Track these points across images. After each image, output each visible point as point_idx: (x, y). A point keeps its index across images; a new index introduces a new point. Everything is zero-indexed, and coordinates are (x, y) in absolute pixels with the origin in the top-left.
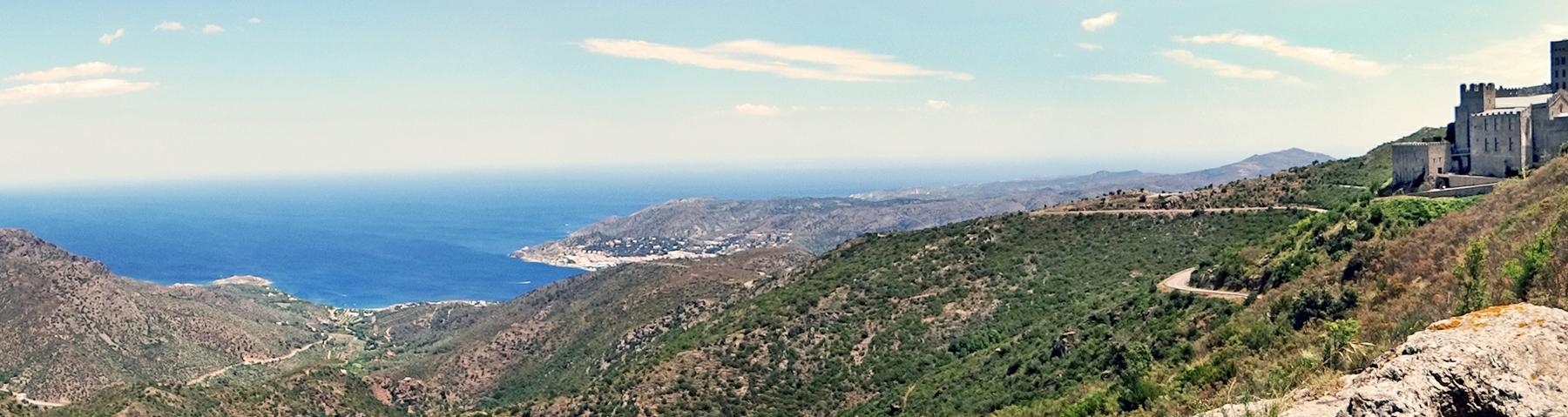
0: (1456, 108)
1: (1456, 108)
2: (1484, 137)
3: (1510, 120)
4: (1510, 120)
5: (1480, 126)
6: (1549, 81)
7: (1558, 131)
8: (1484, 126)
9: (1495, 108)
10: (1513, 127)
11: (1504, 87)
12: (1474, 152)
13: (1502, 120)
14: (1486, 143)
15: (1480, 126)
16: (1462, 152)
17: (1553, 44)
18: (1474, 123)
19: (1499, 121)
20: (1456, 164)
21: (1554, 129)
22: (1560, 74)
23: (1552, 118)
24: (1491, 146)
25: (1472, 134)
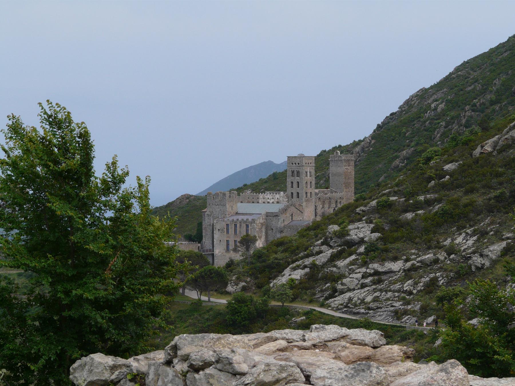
2: (225, 239)
5: (222, 230)
8: (225, 230)
9: (237, 213)
12: (217, 252)
13: (240, 225)
14: (228, 245)
15: (222, 230)
16: (207, 251)
18: (218, 226)
19: (238, 225)
25: (216, 236)
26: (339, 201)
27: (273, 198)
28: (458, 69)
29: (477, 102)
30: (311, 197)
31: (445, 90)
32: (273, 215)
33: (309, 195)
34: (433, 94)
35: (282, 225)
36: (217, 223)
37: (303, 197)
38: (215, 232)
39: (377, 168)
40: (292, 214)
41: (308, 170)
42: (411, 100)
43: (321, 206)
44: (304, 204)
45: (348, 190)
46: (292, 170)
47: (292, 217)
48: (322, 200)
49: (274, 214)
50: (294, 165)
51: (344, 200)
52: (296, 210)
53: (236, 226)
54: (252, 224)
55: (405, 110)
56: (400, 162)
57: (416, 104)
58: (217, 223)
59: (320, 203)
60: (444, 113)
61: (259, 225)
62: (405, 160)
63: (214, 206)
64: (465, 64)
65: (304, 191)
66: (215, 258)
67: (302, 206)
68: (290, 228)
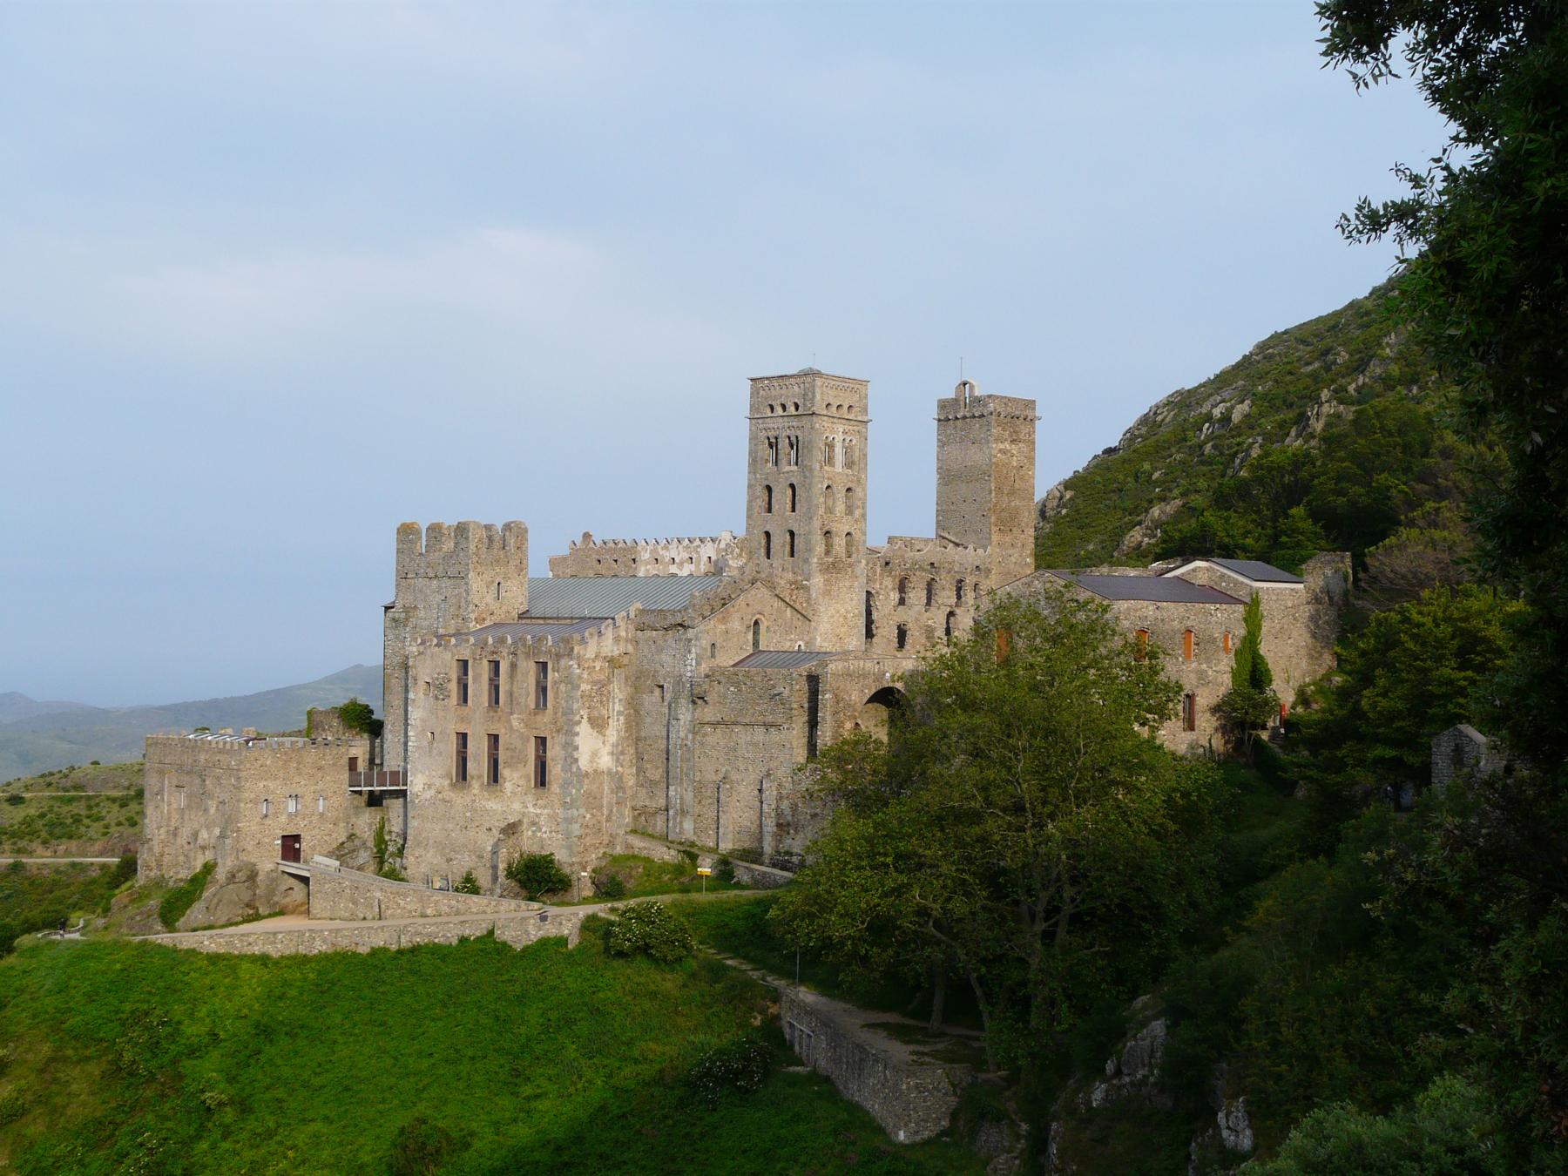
2: (453, 727)
5: (441, 687)
8: (453, 687)
13: (513, 666)
15: (441, 687)
21: (709, 713)
22: (782, 498)
24: (478, 765)
25: (415, 714)
26: (969, 581)
28: (1262, 347)
29: (1350, 384)
31: (1241, 383)
32: (666, 624)
33: (839, 543)
34: (1211, 395)
35: (704, 668)
36: (420, 654)
37: (810, 550)
38: (411, 695)
39: (1082, 552)
40: (756, 623)
41: (839, 438)
42: (1155, 413)
43: (895, 596)
44: (817, 581)
46: (771, 434)
47: (756, 633)
48: (898, 573)
49: (671, 620)
50: (779, 411)
51: (993, 577)
52: (777, 604)
54: (563, 663)
55: (1141, 436)
56: (1145, 535)
57: (1167, 420)
58: (420, 654)
59: (889, 583)
60: (1249, 423)
61: (598, 665)
62: (1156, 529)
63: (421, 582)
64: (1277, 338)
65: (817, 523)
66: (410, 814)
67: (807, 589)
68: (737, 684)
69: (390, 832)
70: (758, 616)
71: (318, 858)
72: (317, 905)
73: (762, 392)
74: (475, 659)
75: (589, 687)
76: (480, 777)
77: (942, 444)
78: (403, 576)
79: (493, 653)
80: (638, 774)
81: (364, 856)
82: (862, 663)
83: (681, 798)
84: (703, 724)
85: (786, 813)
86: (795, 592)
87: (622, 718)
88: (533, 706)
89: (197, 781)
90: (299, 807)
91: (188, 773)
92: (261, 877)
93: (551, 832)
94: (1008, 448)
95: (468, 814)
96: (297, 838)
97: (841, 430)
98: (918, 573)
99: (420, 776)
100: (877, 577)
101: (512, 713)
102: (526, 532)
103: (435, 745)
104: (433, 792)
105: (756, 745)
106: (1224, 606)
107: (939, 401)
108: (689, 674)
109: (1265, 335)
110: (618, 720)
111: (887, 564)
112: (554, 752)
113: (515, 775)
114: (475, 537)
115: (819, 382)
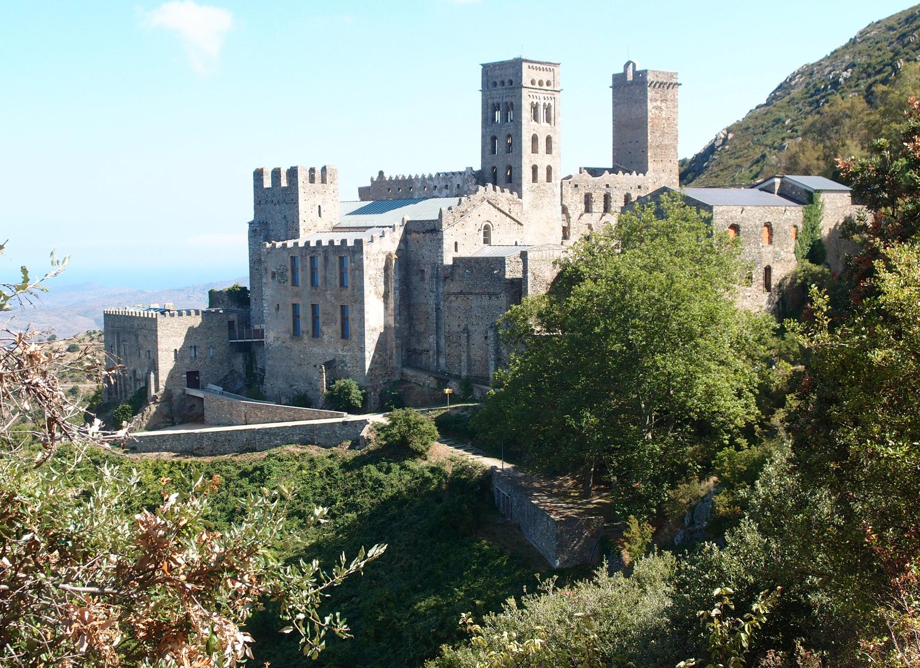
0: (250, 223)
1: (250, 223)
2: (291, 301)
3: (341, 259)
4: (342, 259)
5: (282, 275)
6: (477, 167)
7: (461, 293)
8: (289, 274)
10: (349, 280)
11: (387, 176)
12: (270, 337)
13: (326, 259)
17: (489, 71)
19: (320, 260)
20: (239, 362)
21: (454, 287)
23: (448, 261)
24: (305, 325)
27: (447, 186)
30: (549, 179)
33: (542, 174)
43: (583, 207)
45: (660, 166)
46: (495, 101)
48: (583, 192)
50: (499, 87)
53: (312, 258)
64: (872, 26)
69: (257, 368)
70: (486, 223)
71: (210, 386)
72: (208, 415)
73: (489, 74)
74: (302, 256)
75: (375, 272)
76: (307, 332)
77: (615, 105)
78: (258, 203)
79: (313, 251)
80: (410, 328)
81: (240, 384)
82: (551, 252)
83: (438, 344)
84: (449, 294)
85: (503, 351)
86: (513, 206)
87: (397, 292)
88: (338, 285)
89: (134, 338)
90: (197, 354)
91: (128, 333)
92: (175, 398)
93: (353, 367)
94: (659, 105)
95: (302, 356)
96: (196, 373)
97: (542, 97)
98: (598, 191)
99: (271, 332)
100: (569, 195)
101: (326, 291)
102: (336, 172)
103: (280, 312)
104: (280, 342)
105: (483, 308)
106: (792, 208)
107: (614, 75)
108: (440, 262)
109: (863, 26)
110: (395, 293)
111: (576, 186)
112: (352, 315)
113: (330, 331)
114: (302, 177)
115: (525, 66)
